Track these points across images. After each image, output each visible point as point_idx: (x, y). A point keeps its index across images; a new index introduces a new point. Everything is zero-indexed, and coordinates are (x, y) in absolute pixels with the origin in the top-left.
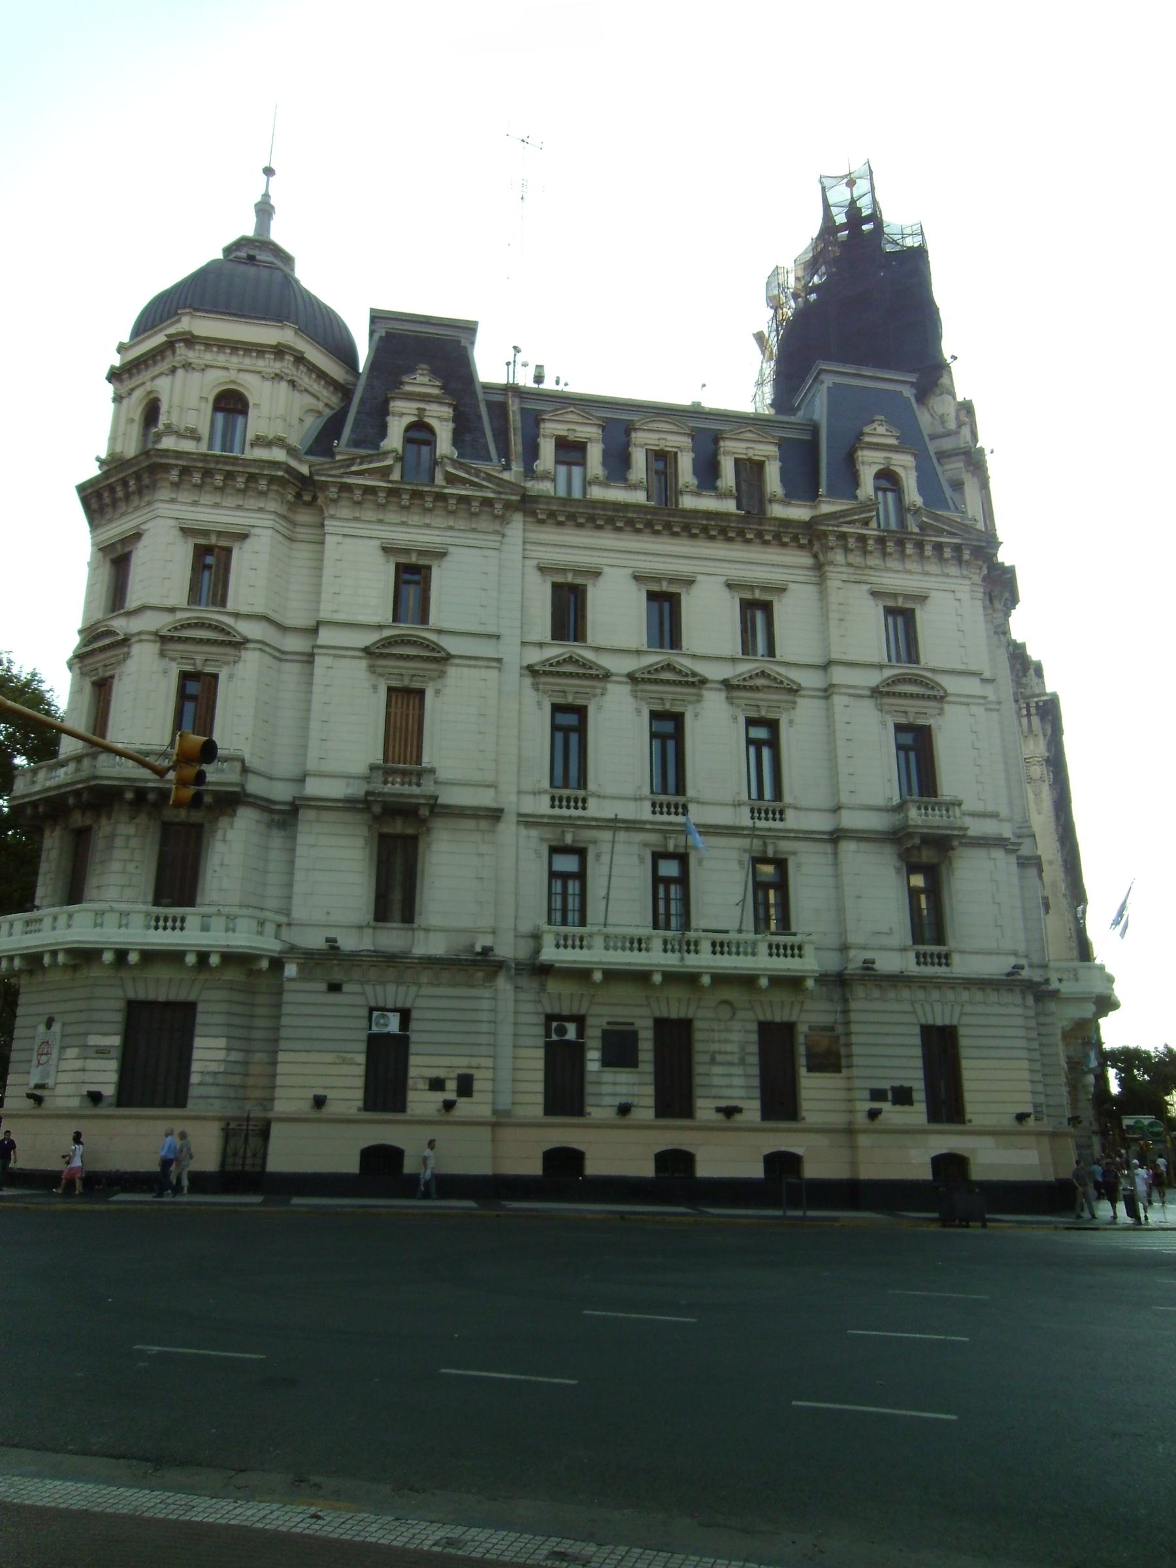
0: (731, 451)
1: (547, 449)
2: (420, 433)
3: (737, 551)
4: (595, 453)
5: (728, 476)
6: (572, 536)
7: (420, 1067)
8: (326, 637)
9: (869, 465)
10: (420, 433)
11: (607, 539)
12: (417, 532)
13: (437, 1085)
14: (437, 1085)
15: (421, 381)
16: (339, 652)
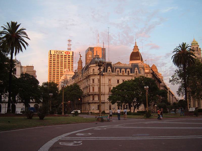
0: (127, 70)
1: (117, 71)
2: (109, 71)
3: (128, 77)
4: (119, 71)
5: (127, 72)
6: (118, 77)
7: (112, 108)
8: (105, 84)
9: (135, 71)
10: (109, 71)
11: (120, 77)
12: (110, 78)
13: (113, 108)
14: (113, 108)
15: (109, 67)
16: (106, 85)
